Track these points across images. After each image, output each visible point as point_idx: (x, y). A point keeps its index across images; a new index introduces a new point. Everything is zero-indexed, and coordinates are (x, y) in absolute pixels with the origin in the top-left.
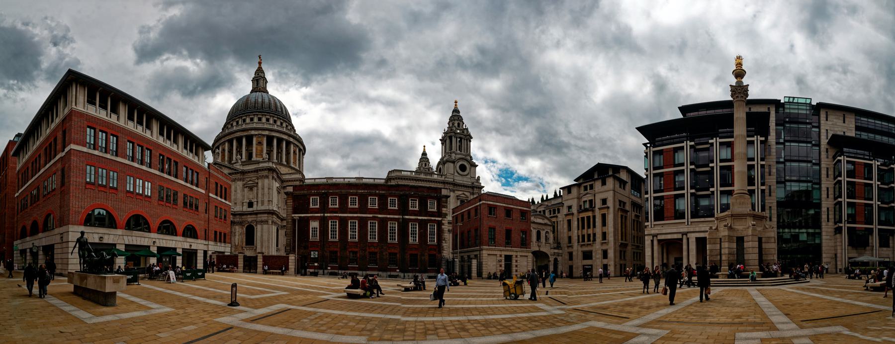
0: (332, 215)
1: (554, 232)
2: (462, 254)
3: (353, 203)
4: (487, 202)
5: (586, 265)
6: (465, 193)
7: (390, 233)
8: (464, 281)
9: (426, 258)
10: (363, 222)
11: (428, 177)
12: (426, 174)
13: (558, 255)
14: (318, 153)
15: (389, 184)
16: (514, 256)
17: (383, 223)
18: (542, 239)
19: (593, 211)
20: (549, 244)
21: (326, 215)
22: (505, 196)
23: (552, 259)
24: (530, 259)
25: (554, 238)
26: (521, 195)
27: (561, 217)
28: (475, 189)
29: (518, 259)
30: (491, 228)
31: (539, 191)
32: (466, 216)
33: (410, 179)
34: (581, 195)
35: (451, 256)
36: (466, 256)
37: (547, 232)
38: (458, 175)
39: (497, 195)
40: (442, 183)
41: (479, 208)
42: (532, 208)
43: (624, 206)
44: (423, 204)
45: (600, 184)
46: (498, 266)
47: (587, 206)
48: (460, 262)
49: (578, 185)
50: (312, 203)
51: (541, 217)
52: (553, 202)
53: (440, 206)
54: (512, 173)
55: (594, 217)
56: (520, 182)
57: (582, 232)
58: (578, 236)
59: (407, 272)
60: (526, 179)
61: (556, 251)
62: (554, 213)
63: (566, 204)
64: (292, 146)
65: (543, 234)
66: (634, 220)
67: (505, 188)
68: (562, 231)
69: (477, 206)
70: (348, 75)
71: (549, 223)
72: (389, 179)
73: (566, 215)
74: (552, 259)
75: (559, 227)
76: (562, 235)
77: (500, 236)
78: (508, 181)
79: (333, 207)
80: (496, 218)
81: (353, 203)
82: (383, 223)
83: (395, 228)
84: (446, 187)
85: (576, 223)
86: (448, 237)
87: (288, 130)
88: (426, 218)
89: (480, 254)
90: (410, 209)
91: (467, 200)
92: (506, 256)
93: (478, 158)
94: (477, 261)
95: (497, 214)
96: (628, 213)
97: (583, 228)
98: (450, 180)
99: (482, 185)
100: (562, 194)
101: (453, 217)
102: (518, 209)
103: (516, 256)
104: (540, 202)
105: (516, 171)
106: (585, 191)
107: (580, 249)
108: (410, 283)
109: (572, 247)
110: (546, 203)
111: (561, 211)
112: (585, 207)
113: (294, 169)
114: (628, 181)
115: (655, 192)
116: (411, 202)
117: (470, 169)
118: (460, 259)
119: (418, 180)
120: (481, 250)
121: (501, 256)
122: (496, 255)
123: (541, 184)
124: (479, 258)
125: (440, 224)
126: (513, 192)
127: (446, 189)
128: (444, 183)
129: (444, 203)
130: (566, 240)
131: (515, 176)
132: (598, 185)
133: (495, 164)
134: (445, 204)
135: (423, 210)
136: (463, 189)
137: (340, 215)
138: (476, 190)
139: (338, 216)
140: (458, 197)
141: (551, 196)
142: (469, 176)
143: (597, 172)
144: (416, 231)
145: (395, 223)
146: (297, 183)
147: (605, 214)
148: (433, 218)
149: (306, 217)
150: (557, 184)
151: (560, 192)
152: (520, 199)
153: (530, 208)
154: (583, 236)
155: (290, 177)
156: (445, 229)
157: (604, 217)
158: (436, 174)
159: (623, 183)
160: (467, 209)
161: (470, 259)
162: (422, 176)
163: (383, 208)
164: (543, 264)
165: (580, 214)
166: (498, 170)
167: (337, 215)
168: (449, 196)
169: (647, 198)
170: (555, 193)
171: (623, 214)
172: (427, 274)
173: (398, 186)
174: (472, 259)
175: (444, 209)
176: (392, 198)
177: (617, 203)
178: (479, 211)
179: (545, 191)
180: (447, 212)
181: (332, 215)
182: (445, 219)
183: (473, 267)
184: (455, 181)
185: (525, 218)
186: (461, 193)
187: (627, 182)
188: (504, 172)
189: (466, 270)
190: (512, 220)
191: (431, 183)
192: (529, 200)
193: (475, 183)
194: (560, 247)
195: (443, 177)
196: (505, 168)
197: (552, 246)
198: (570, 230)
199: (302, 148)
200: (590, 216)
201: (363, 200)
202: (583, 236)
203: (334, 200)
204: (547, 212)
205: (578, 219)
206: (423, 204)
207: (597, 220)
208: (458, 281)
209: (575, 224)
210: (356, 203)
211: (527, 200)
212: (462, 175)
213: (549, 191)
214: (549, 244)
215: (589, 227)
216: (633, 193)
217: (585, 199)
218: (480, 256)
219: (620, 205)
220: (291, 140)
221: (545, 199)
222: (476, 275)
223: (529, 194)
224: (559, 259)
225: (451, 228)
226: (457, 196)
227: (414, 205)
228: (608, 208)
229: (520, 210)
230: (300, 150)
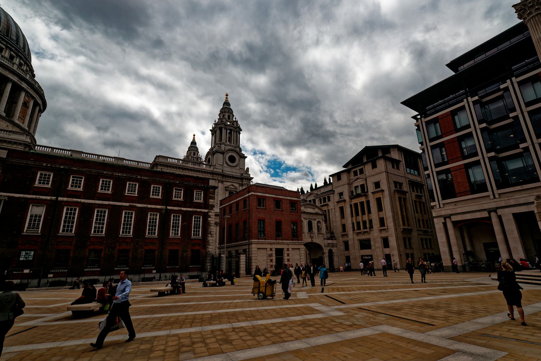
0: (70, 199)
1: (326, 221)
2: (230, 249)
3: (106, 187)
4: (255, 194)
5: (365, 256)
6: (234, 184)
7: (149, 226)
8: (231, 279)
9: (189, 254)
10: (115, 213)
11: (196, 167)
12: (194, 163)
13: (333, 246)
14: (62, 115)
15: (155, 169)
16: (285, 250)
17: (142, 214)
18: (313, 229)
19: (366, 196)
20: (322, 234)
21: (60, 199)
22: (273, 187)
23: (326, 250)
24: (303, 252)
25: (327, 227)
26: (290, 186)
27: (333, 205)
28: (245, 181)
29: (290, 252)
30: (261, 220)
31: (307, 180)
32: (234, 209)
33: (176, 168)
34: (352, 181)
35: (217, 251)
36: (234, 251)
37: (319, 222)
38: (227, 166)
39: (266, 186)
40: (210, 173)
41: (248, 199)
42: (302, 197)
43: (401, 187)
44: (189, 195)
45: (371, 167)
46: (269, 261)
47: (359, 191)
48: (227, 258)
49: (348, 172)
50: (39, 180)
51: (311, 207)
52: (323, 191)
53: (206, 198)
54: (280, 164)
55: (368, 202)
56: (288, 172)
57: (356, 219)
58: (353, 224)
59: (164, 272)
60: (294, 169)
61: (330, 241)
62: (325, 201)
63: (337, 191)
64: (23, 95)
65: (314, 224)
66: (415, 202)
67: (274, 178)
68: (334, 219)
69: (246, 197)
70: (119, 44)
71: (321, 213)
72: (155, 164)
73: (338, 202)
74: (326, 250)
75: (331, 216)
76: (335, 224)
77: (270, 229)
78: (277, 171)
79: (74, 189)
80: (266, 209)
81: (106, 187)
82: (142, 214)
83: (156, 219)
84: (214, 178)
85: (349, 210)
86: (215, 230)
87: (22, 70)
88: (191, 209)
89: (249, 248)
90: (174, 199)
91: (235, 191)
92: (277, 250)
93: (247, 150)
94: (246, 256)
95: (266, 205)
96: (407, 194)
97: (357, 214)
98: (219, 171)
99: (251, 176)
100: (332, 182)
101: (221, 209)
102: (287, 199)
103: (288, 249)
104: (309, 191)
105: (284, 162)
106: (355, 176)
107: (357, 238)
108: (167, 286)
109: (346, 235)
110: (316, 192)
111: (331, 199)
112: (358, 193)
113: (18, 126)
114: (401, 160)
115: (437, 166)
116: (176, 192)
117: (239, 160)
118: (227, 255)
119: (185, 169)
120: (250, 244)
121: (271, 249)
122: (267, 248)
123: (309, 172)
124: (248, 253)
125: (206, 216)
126: (282, 182)
127: (215, 179)
128: (212, 173)
129: (211, 194)
130: (340, 229)
131: (283, 167)
132: (368, 168)
133: (264, 156)
134: (213, 195)
136: (232, 180)
137: (83, 201)
138: (245, 182)
139: (81, 202)
140: (226, 189)
141: (320, 184)
142: (238, 168)
143: (365, 156)
144: (179, 223)
145: (156, 215)
146: (20, 148)
147: (380, 198)
149: (23, 198)
150: (326, 172)
151: (330, 179)
152: (289, 189)
153: (300, 198)
154: (358, 223)
155: (7, 136)
156: (211, 222)
157: (379, 201)
158: (204, 164)
159: (395, 163)
160: (235, 201)
161: (238, 254)
162: (190, 165)
163: (144, 196)
164: (317, 257)
165: (353, 200)
166: (267, 161)
167: (79, 200)
168: (217, 187)
169: (428, 175)
170: (325, 180)
171: (400, 196)
172: (188, 274)
173: (162, 173)
174: (240, 254)
175: (211, 201)
176: (155, 186)
177: (392, 186)
178: (247, 203)
179: (313, 180)
180: (214, 204)
181: (70, 199)
182: (212, 211)
183: (241, 263)
184: (224, 172)
185: (295, 208)
186: (229, 184)
187: (401, 161)
188: (273, 163)
189: (234, 267)
190: (282, 211)
191: (198, 173)
192: (298, 190)
193: (244, 175)
194: (334, 237)
195: (212, 167)
196: (273, 159)
197: (325, 237)
198: (344, 218)
199: (40, 102)
200: (363, 202)
201: (119, 186)
202: (358, 223)
203: (77, 180)
204: (317, 200)
205: (351, 206)
206: (189, 195)
207: (371, 205)
208: (224, 280)
209: (347, 211)
210: (109, 187)
211: (295, 190)
212: (231, 166)
213: (318, 179)
214: (322, 234)
215: (363, 213)
216: (408, 171)
217: (356, 184)
218: (249, 251)
219: (396, 187)
220: (24, 85)
221: (314, 187)
222: (244, 272)
223: (298, 183)
224: (334, 250)
225: (218, 221)
226: (226, 187)
227: (178, 195)
228: (382, 191)
229: (289, 200)
230: (36, 104)
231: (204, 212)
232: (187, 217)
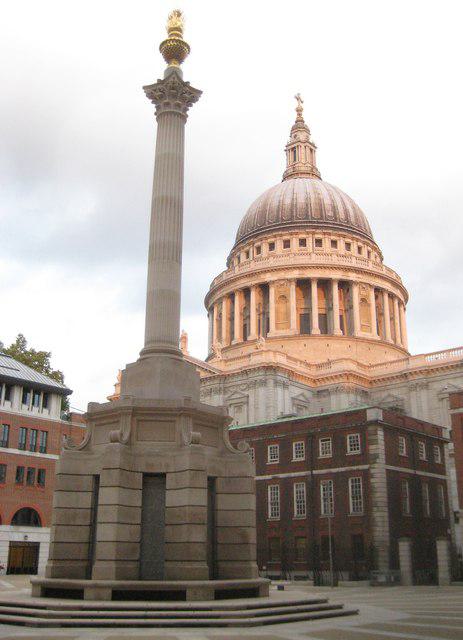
44: (339, 446)
88: (343, 469)
125: (367, 475)
135: (339, 457)
148: (355, 468)
182: (376, 465)
206: (339, 446)
227: (325, 450)
231: (364, 470)
232: (340, 481)
